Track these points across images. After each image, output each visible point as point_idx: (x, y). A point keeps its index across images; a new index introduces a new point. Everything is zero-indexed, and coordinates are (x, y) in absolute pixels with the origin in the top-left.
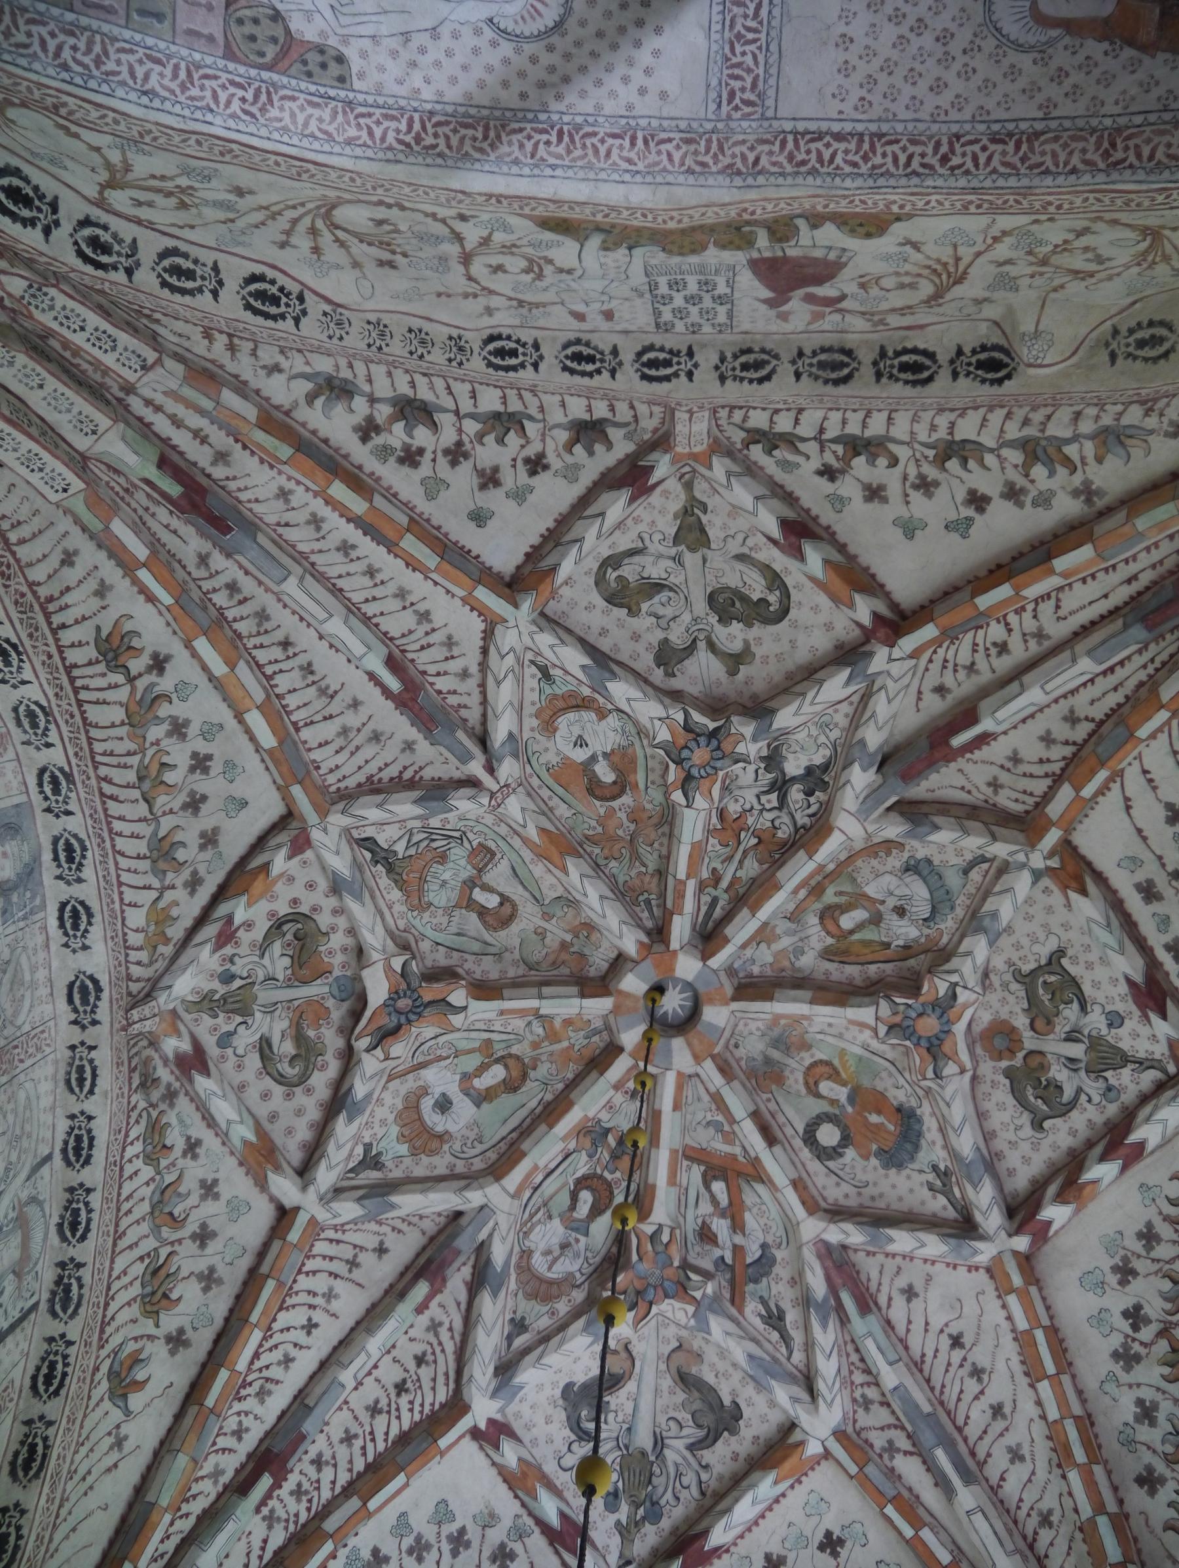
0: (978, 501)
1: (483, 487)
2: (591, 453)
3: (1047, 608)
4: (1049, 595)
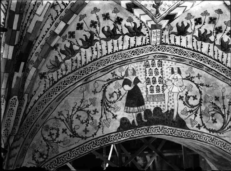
0: (80, 27)
1: (215, 19)
2: (182, 23)
3: (54, 16)
4: (55, 19)
